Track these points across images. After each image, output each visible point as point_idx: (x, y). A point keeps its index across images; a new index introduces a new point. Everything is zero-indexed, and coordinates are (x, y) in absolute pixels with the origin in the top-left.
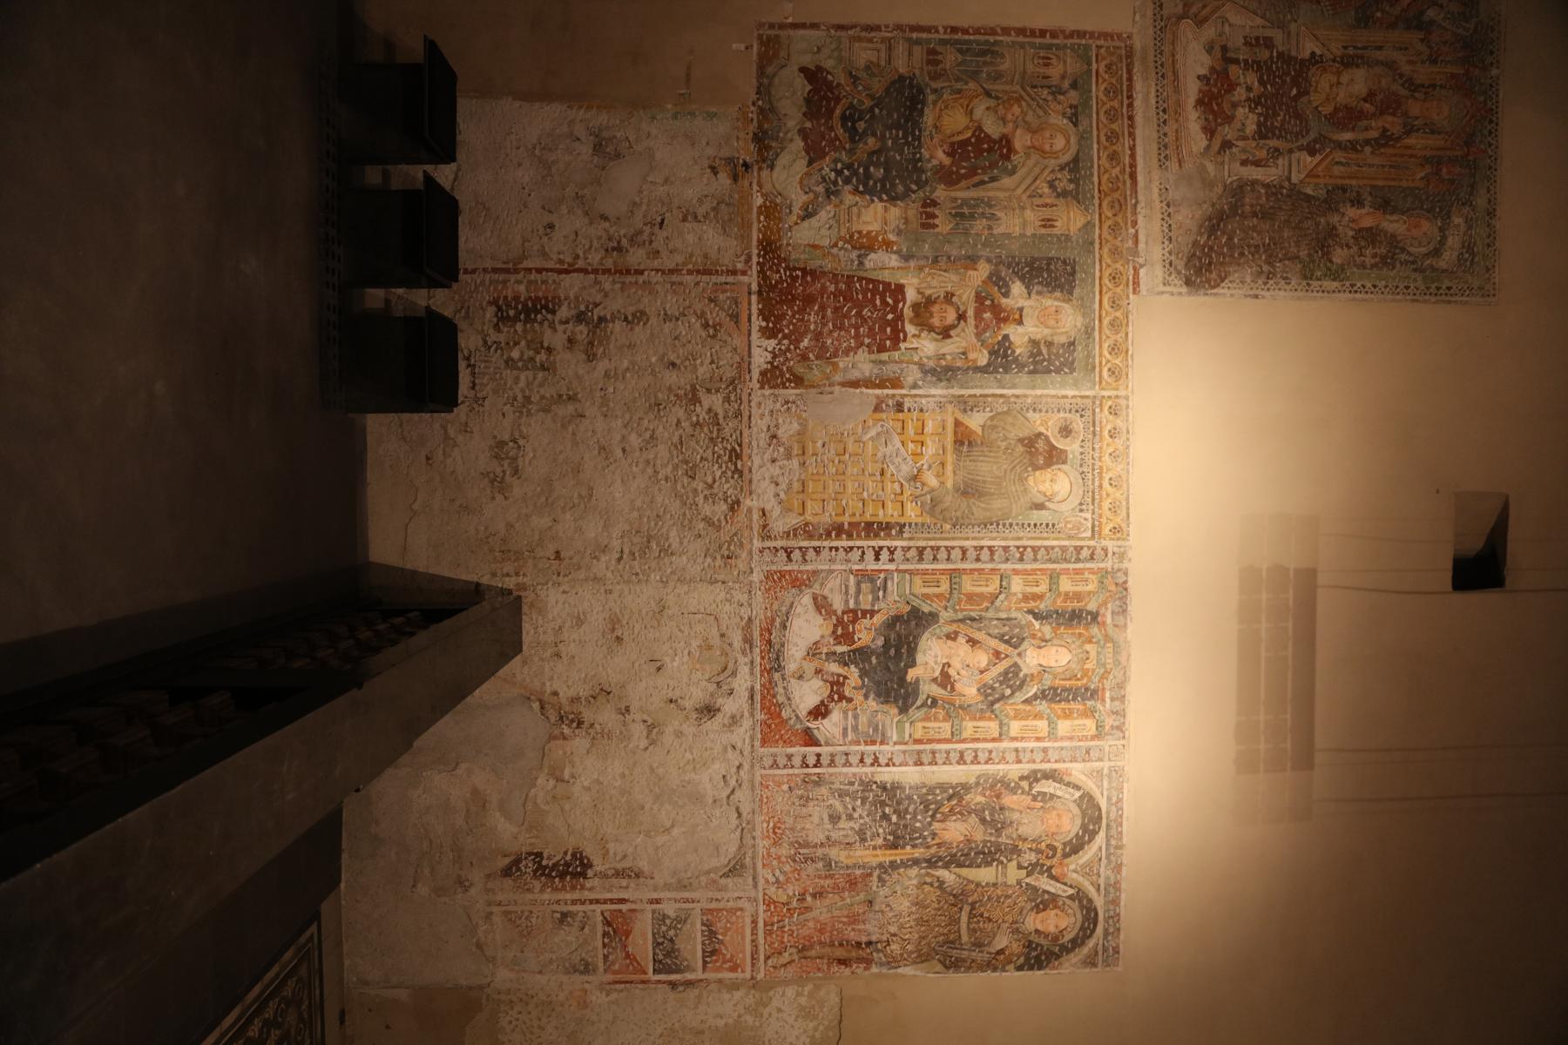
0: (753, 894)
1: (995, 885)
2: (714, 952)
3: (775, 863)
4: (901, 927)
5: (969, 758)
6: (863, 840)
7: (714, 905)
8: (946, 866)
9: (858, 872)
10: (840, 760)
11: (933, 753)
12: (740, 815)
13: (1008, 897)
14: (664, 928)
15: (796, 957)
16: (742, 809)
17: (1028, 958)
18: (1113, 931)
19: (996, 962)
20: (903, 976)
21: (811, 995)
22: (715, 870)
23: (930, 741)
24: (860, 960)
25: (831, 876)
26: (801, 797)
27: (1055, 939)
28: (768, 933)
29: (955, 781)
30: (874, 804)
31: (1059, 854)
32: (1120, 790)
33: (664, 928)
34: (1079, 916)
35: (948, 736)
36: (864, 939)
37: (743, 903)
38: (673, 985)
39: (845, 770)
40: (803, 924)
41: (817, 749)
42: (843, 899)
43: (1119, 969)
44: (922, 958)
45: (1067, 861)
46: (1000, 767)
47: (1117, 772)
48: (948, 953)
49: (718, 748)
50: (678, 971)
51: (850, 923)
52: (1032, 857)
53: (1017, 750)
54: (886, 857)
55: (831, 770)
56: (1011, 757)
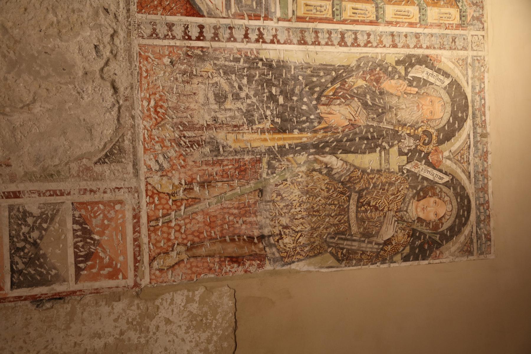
0: (133, 183)
1: (379, 171)
2: (89, 256)
3: (158, 147)
4: (293, 218)
5: (349, 40)
6: (251, 122)
7: (87, 198)
8: (333, 153)
9: (247, 158)
10: (224, 34)
11: (316, 32)
12: (115, 90)
13: (391, 184)
14: (25, 229)
15: (184, 256)
16: (118, 84)
17: (412, 249)
18: (484, 219)
19: (383, 254)
20: (298, 272)
21: (202, 301)
22: (88, 156)
23: (313, 20)
24: (254, 256)
25: (220, 163)
26: (184, 73)
27: (436, 227)
28: (152, 230)
29: (337, 63)
30: (260, 83)
31: (434, 141)
32: (482, 80)
33: (25, 229)
34: (455, 203)
35: (329, 15)
36: (256, 233)
37: (121, 195)
38: (37, 301)
39: (230, 45)
40: (191, 218)
41: (200, 20)
42: (232, 188)
43: (492, 257)
44: (315, 251)
45: (441, 147)
46: (378, 50)
47: (479, 62)
48: (339, 245)
49: (88, 11)
50: (45, 282)
51: (240, 216)
52: (409, 143)
53: (392, 35)
54: (274, 141)
55: (216, 44)
56: (387, 41)
